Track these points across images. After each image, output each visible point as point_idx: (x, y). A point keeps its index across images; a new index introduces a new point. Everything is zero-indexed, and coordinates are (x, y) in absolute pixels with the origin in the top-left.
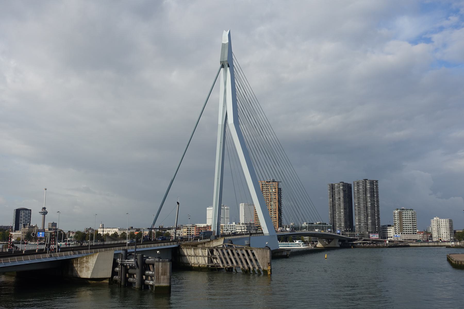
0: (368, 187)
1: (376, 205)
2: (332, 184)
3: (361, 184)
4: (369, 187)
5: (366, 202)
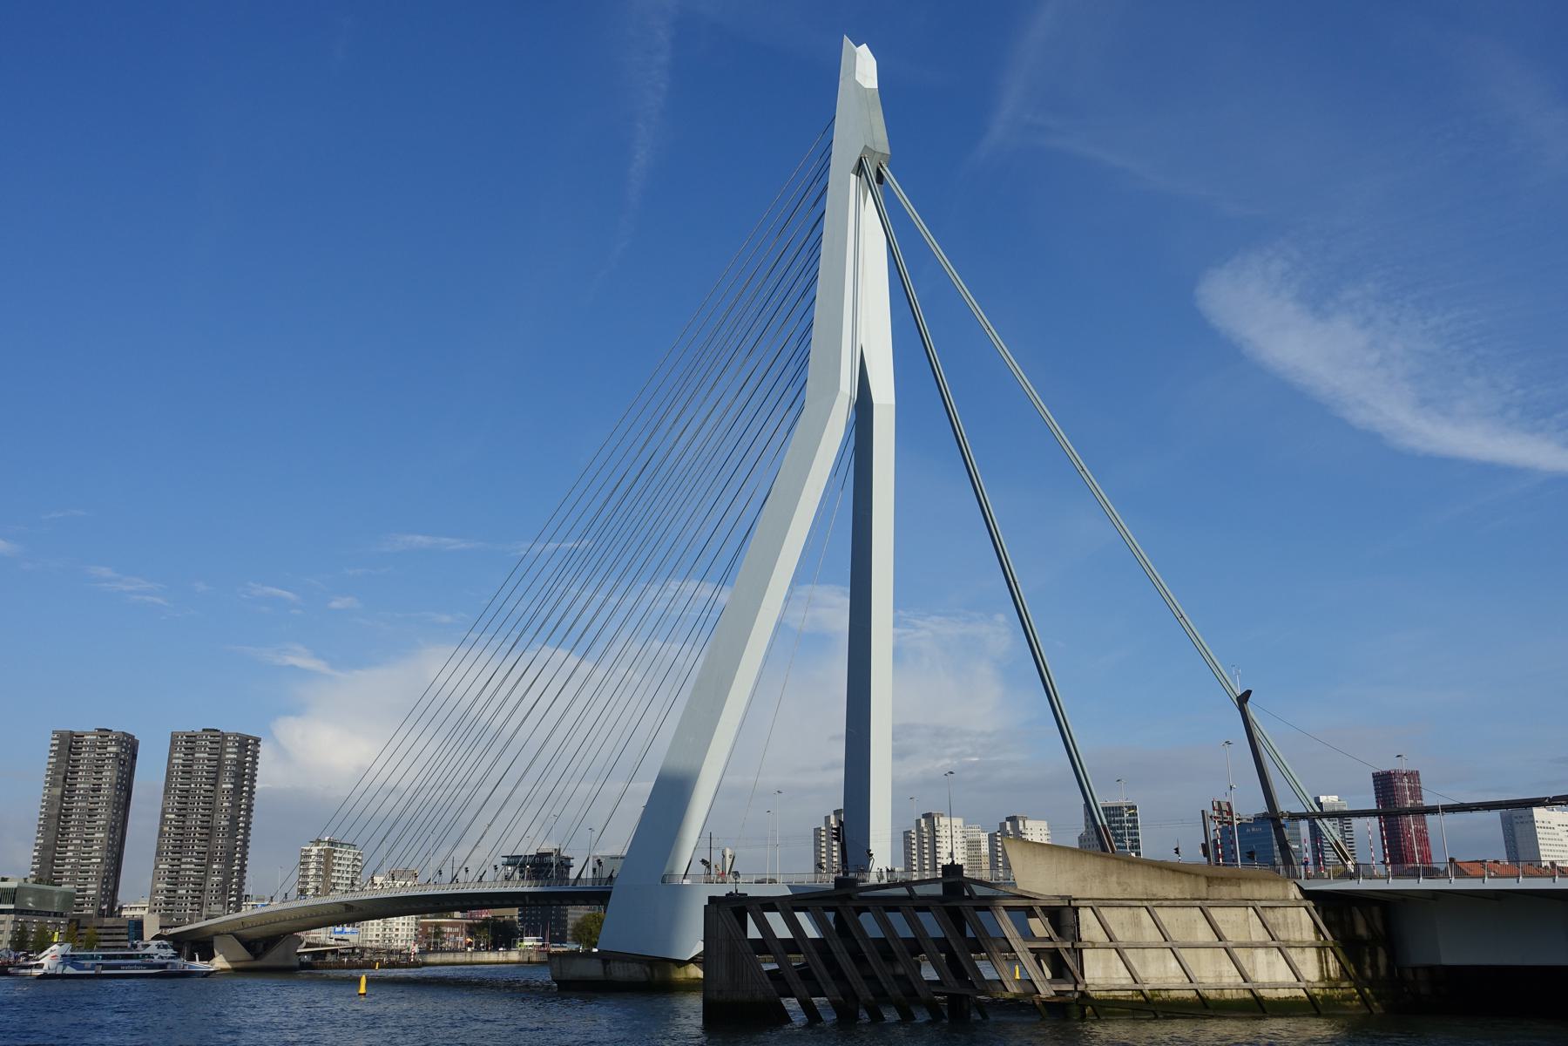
0: (227, 756)
1: (242, 822)
2: (72, 733)
3: (205, 746)
4: (233, 756)
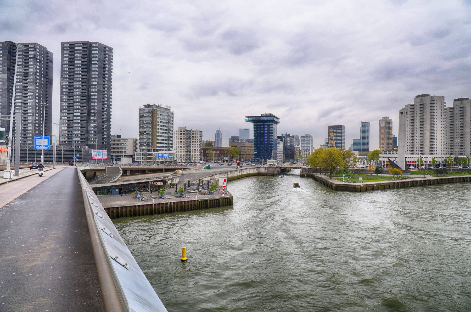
5: (89, 86)
